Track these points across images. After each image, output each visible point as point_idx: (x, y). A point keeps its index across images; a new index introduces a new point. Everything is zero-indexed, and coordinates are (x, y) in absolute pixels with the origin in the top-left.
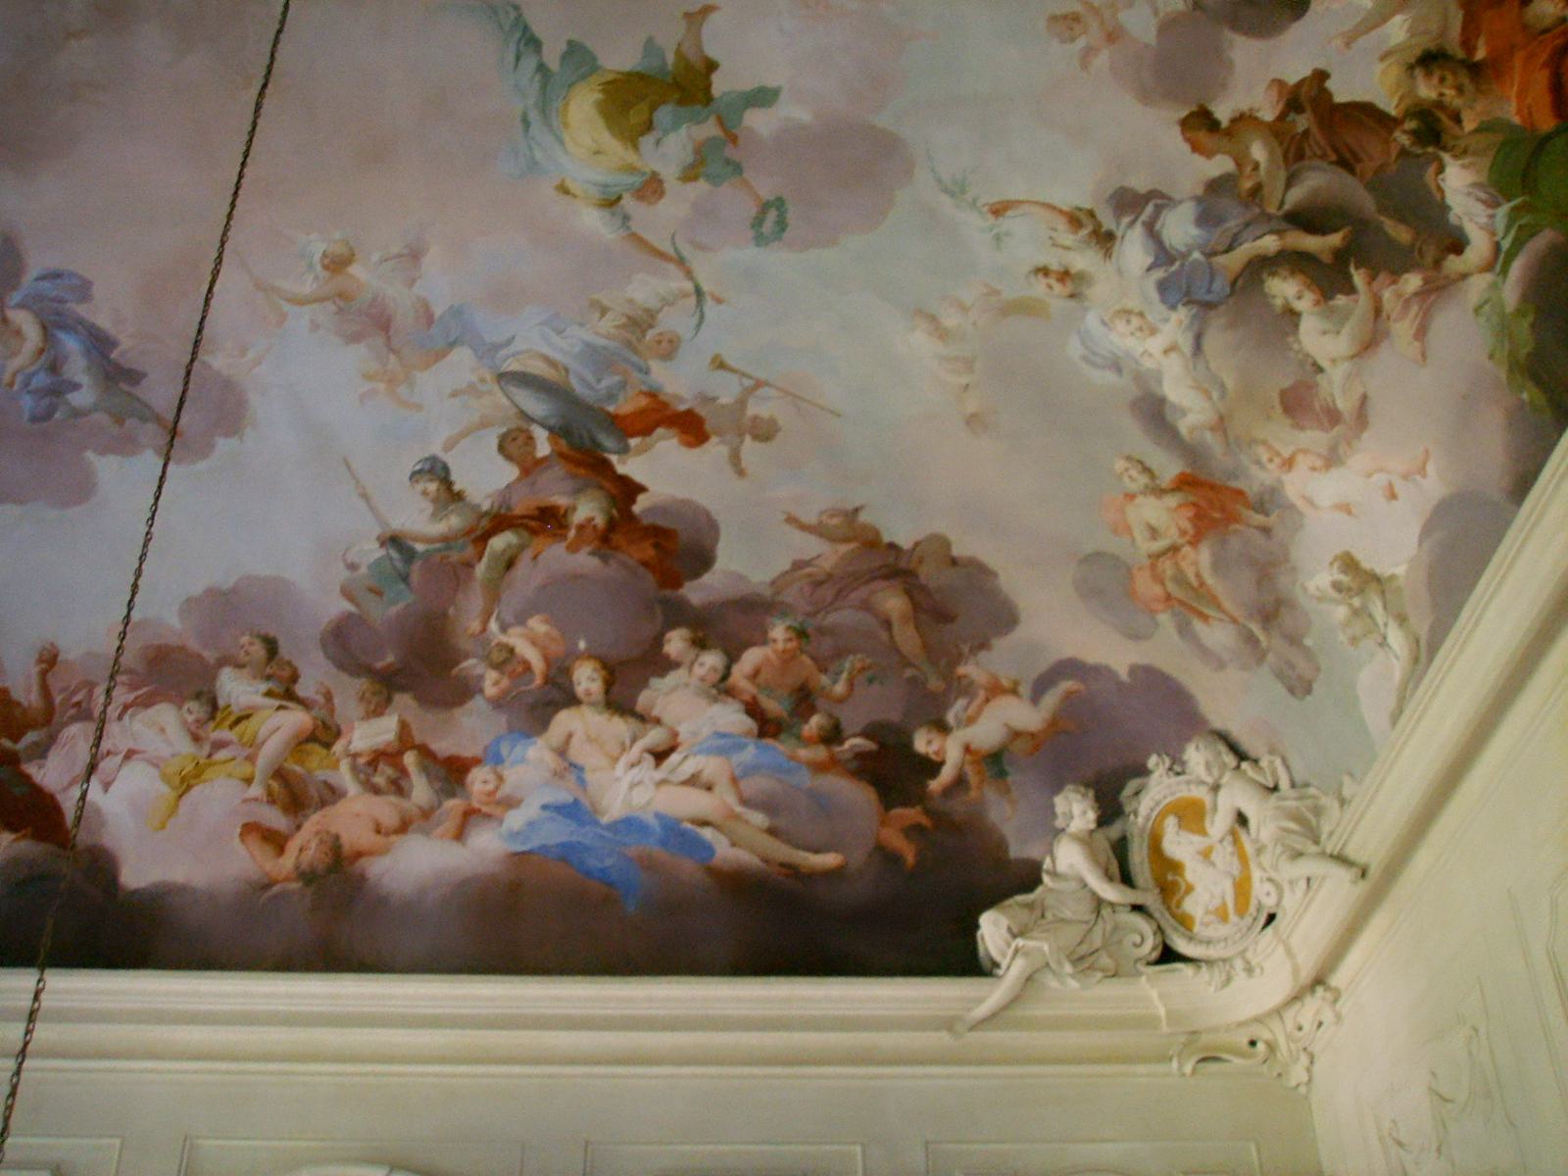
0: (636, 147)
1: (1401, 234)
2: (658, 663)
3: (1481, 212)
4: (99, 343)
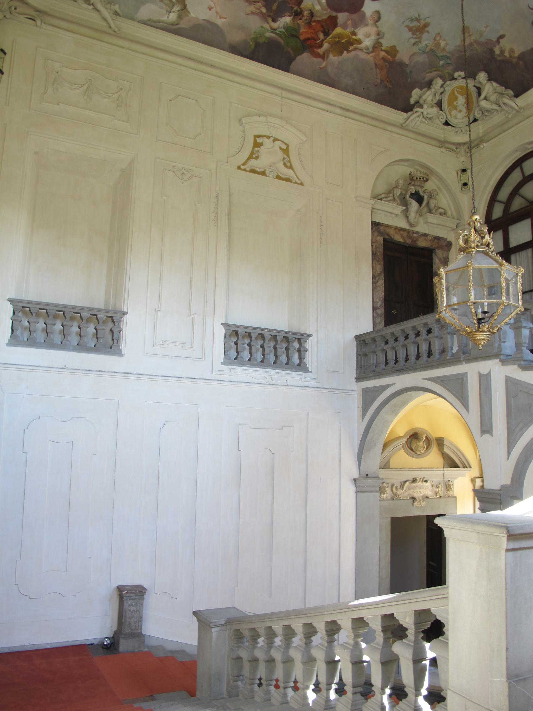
1: (274, 7)
3: (282, 25)
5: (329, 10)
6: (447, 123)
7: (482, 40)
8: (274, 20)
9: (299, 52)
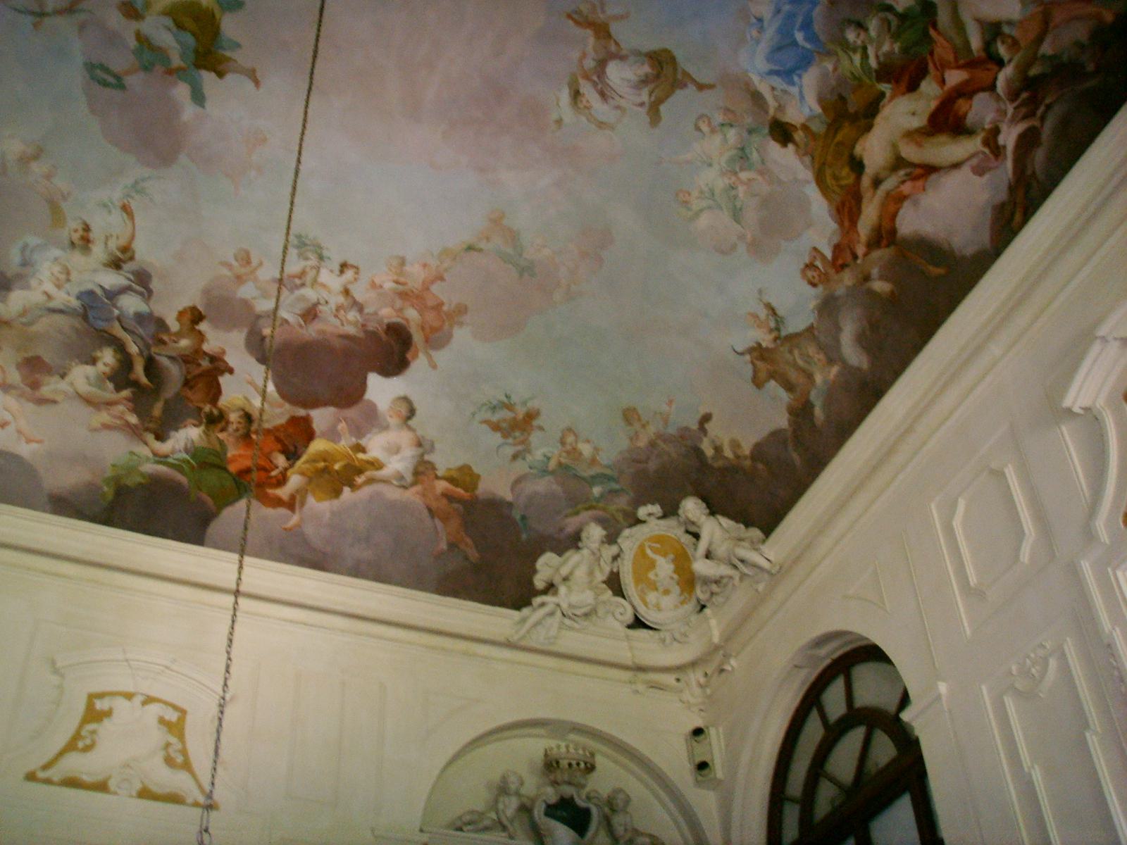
1: (157, 410)
3: (181, 445)
5: (287, 406)
6: (638, 623)
7: (672, 430)
8: (160, 437)
9: (225, 499)
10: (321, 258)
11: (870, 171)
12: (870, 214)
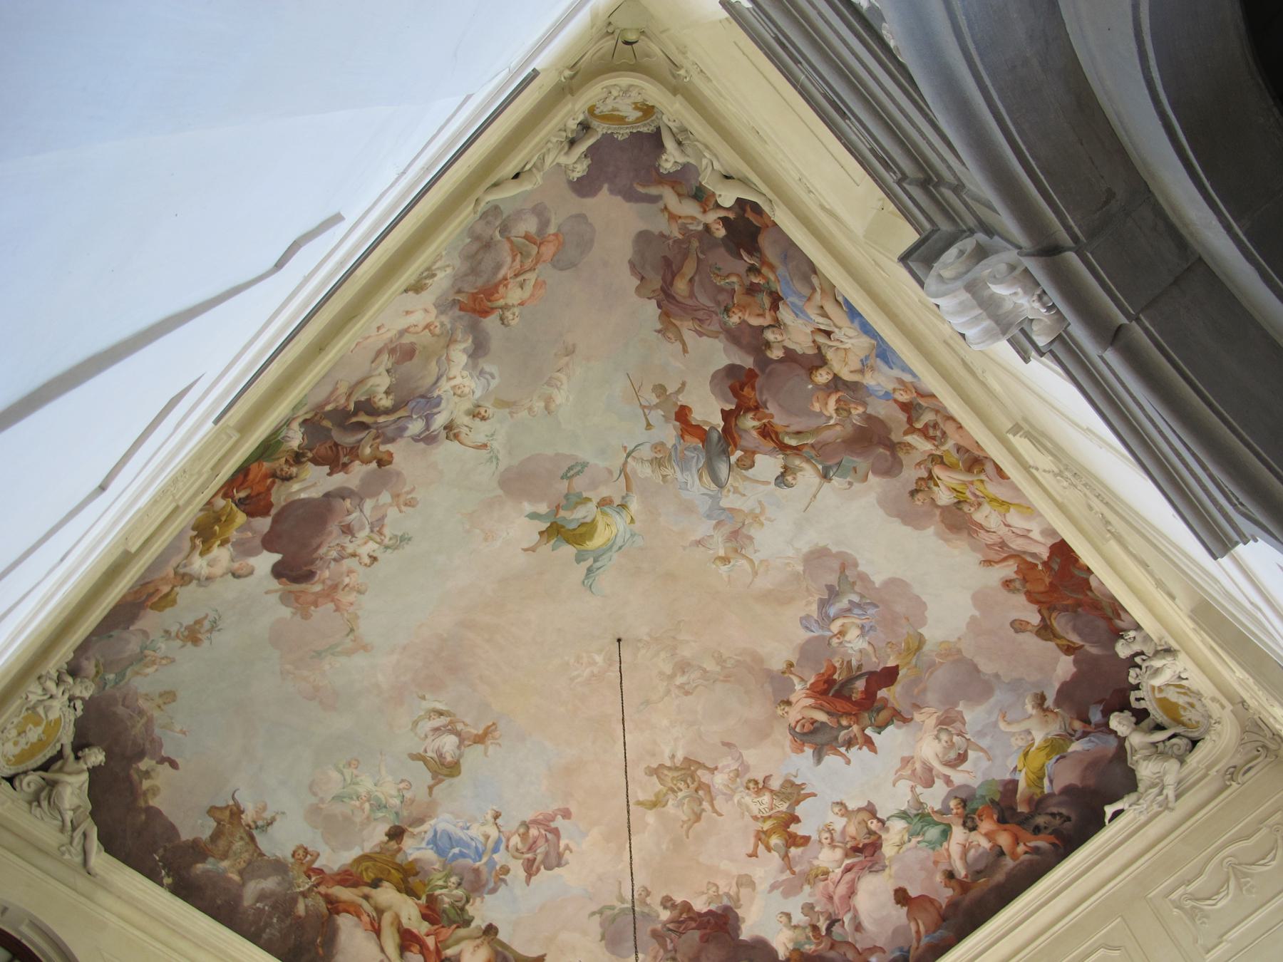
0: (593, 520)
1: (327, 423)
2: (791, 357)
3: (291, 434)
4: (823, 604)
5: (283, 504)
7: (157, 732)
10: (387, 547)
11: (373, 892)
12: (344, 894)
